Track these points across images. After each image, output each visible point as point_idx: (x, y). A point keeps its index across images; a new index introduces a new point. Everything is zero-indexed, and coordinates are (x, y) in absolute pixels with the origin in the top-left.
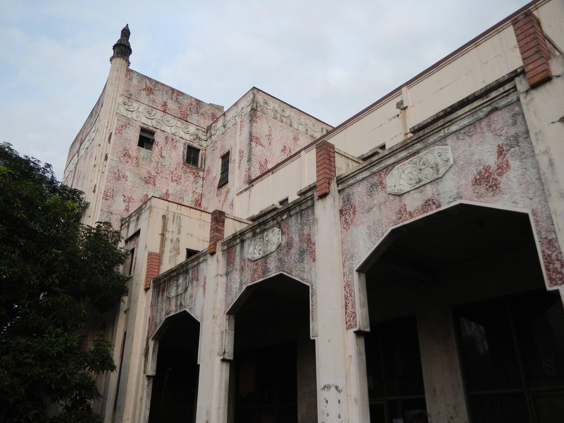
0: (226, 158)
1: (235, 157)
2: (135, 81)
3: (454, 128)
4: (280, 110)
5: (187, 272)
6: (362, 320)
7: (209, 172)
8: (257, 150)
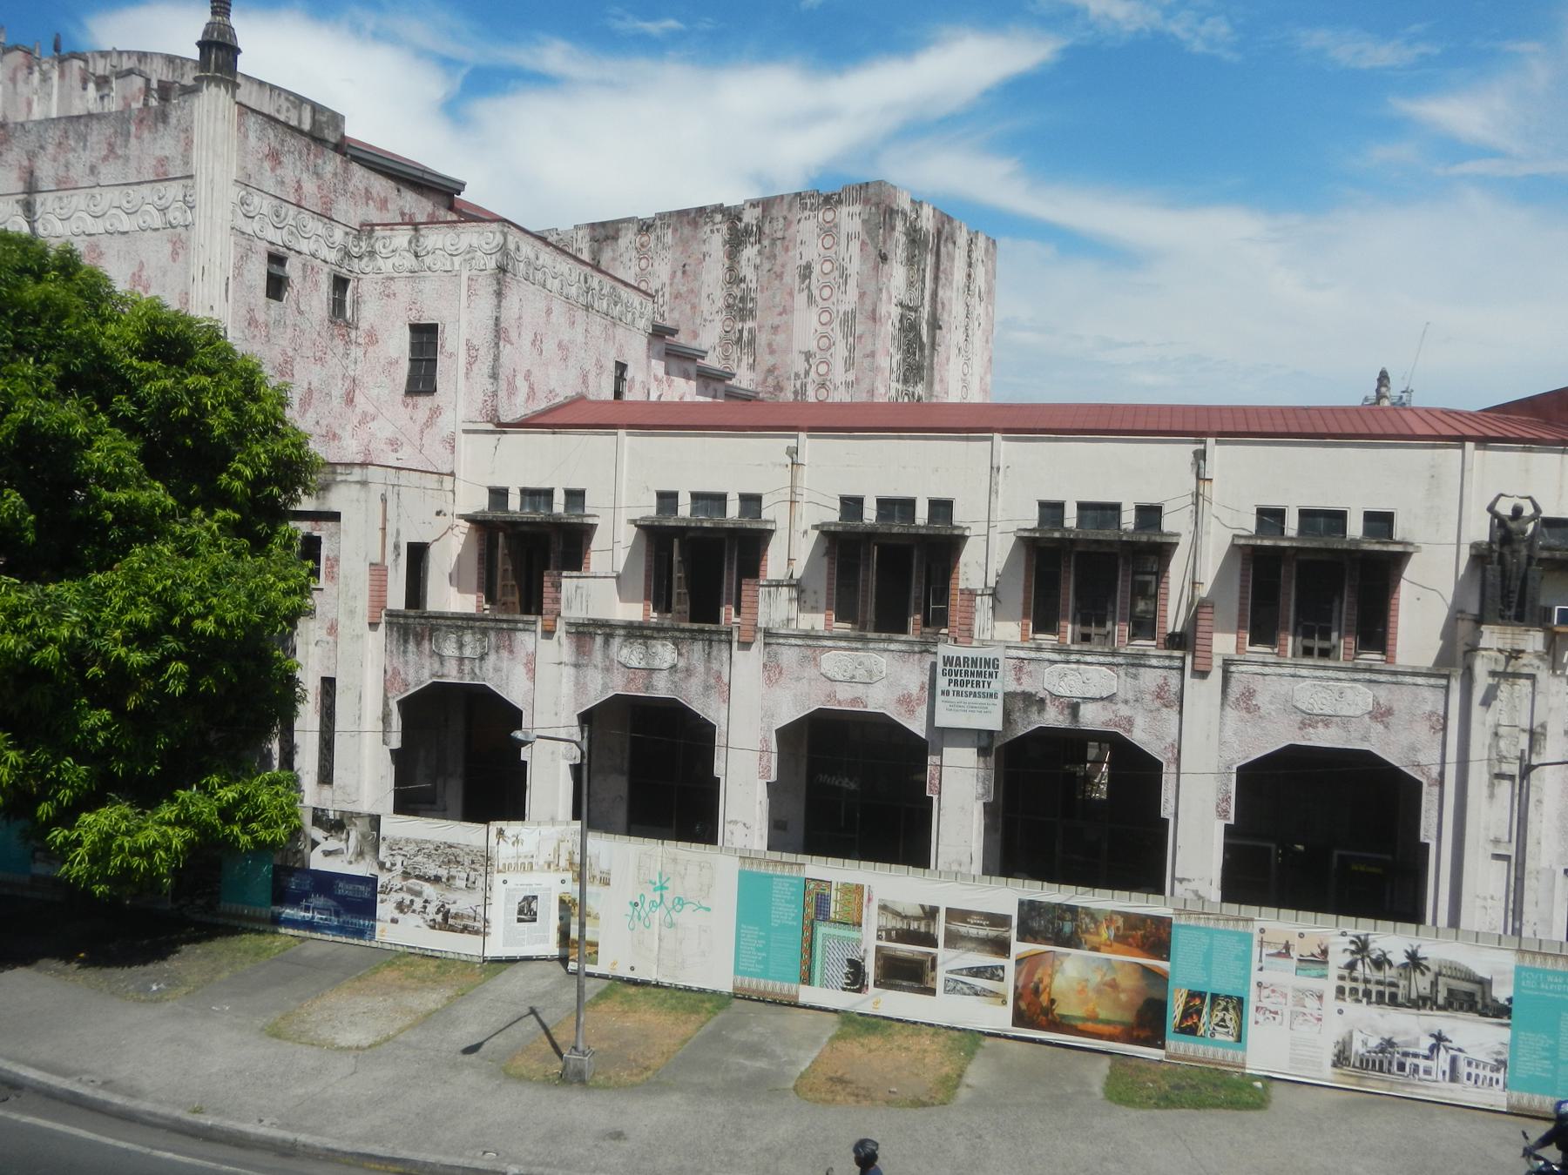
0: (425, 337)
1: (452, 344)
2: (252, 140)
3: (892, 646)
4: (532, 256)
5: (484, 632)
6: (773, 778)
7: (372, 338)
8: (506, 350)
